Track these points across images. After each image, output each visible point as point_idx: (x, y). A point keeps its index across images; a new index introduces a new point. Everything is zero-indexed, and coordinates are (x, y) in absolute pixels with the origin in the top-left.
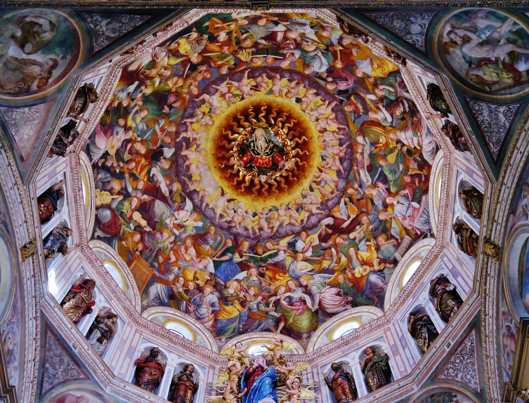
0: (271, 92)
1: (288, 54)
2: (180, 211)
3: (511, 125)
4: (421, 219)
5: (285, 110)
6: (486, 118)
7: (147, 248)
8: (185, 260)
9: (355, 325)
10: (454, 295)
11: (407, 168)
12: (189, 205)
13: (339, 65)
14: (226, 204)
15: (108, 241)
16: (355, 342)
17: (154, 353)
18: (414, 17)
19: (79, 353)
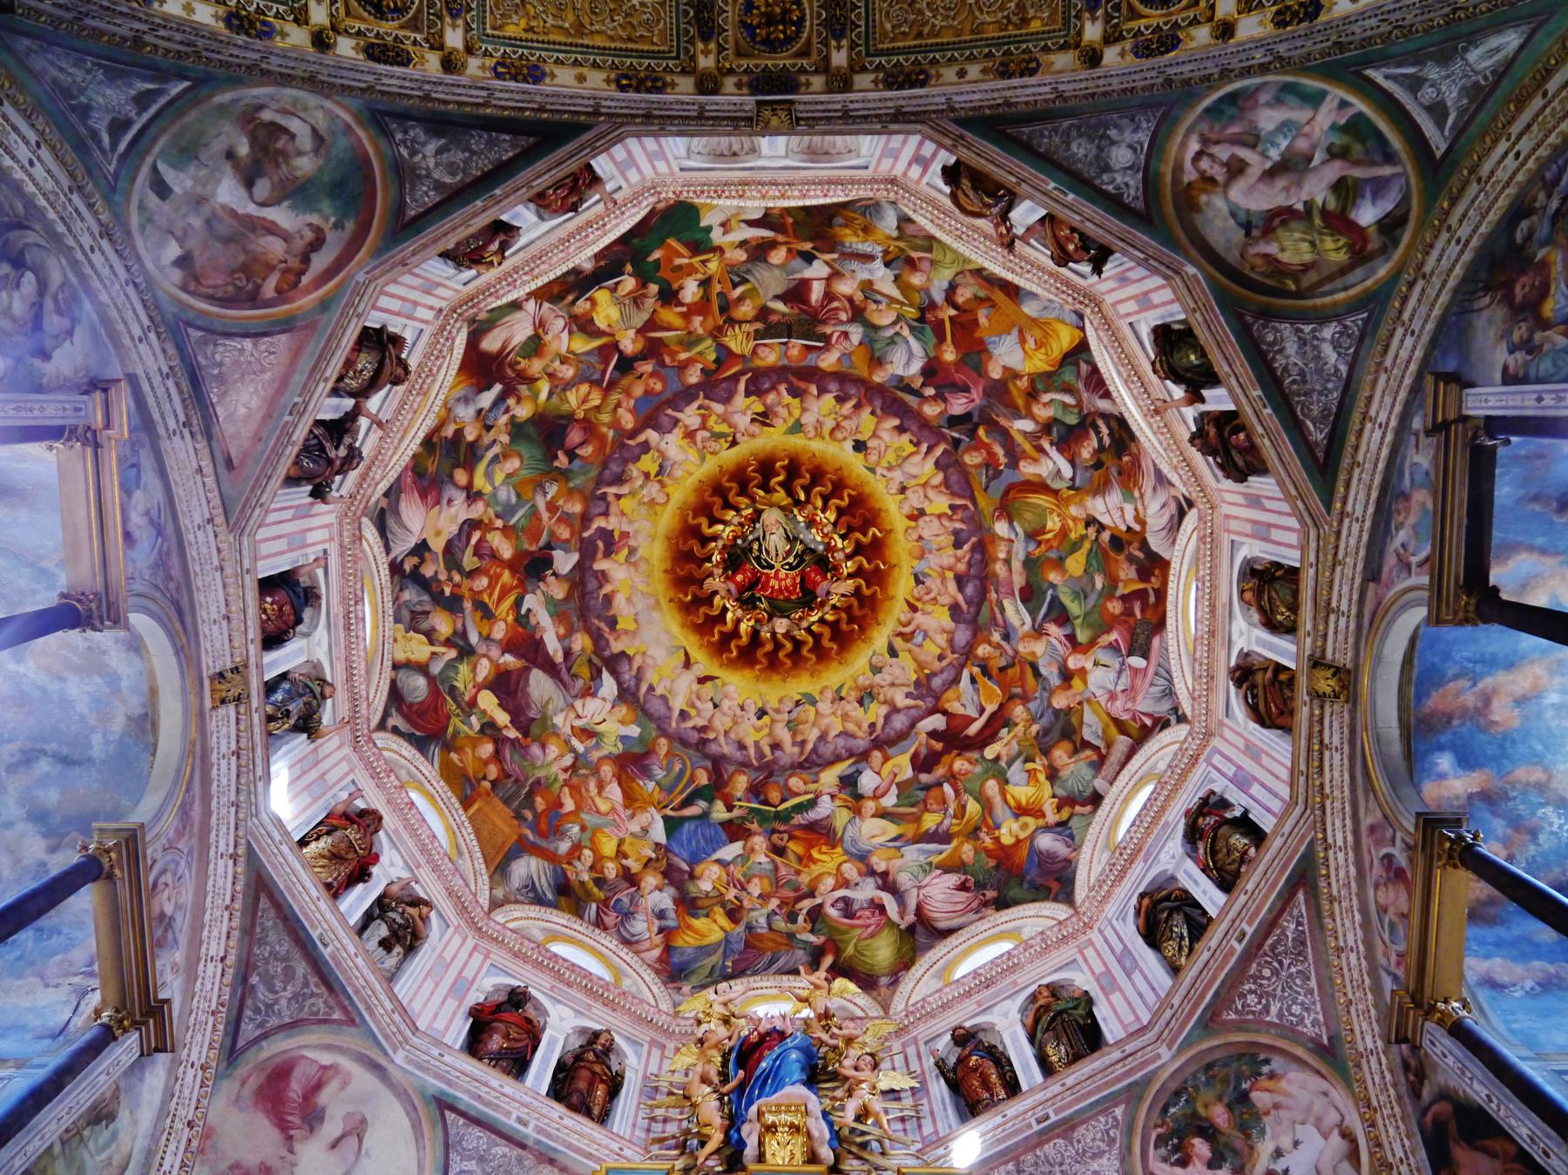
0: (797, 427)
1: (836, 335)
2: (589, 700)
3: (1352, 367)
4: (1154, 690)
5: (829, 469)
6: (1293, 360)
7: (508, 776)
8: (598, 812)
9: (1005, 946)
10: (1245, 824)
11: (1113, 582)
12: (609, 686)
13: (949, 355)
14: (695, 686)
15: (421, 744)
16: (1009, 980)
17: (517, 998)
18: (1116, 127)
19: (334, 957)
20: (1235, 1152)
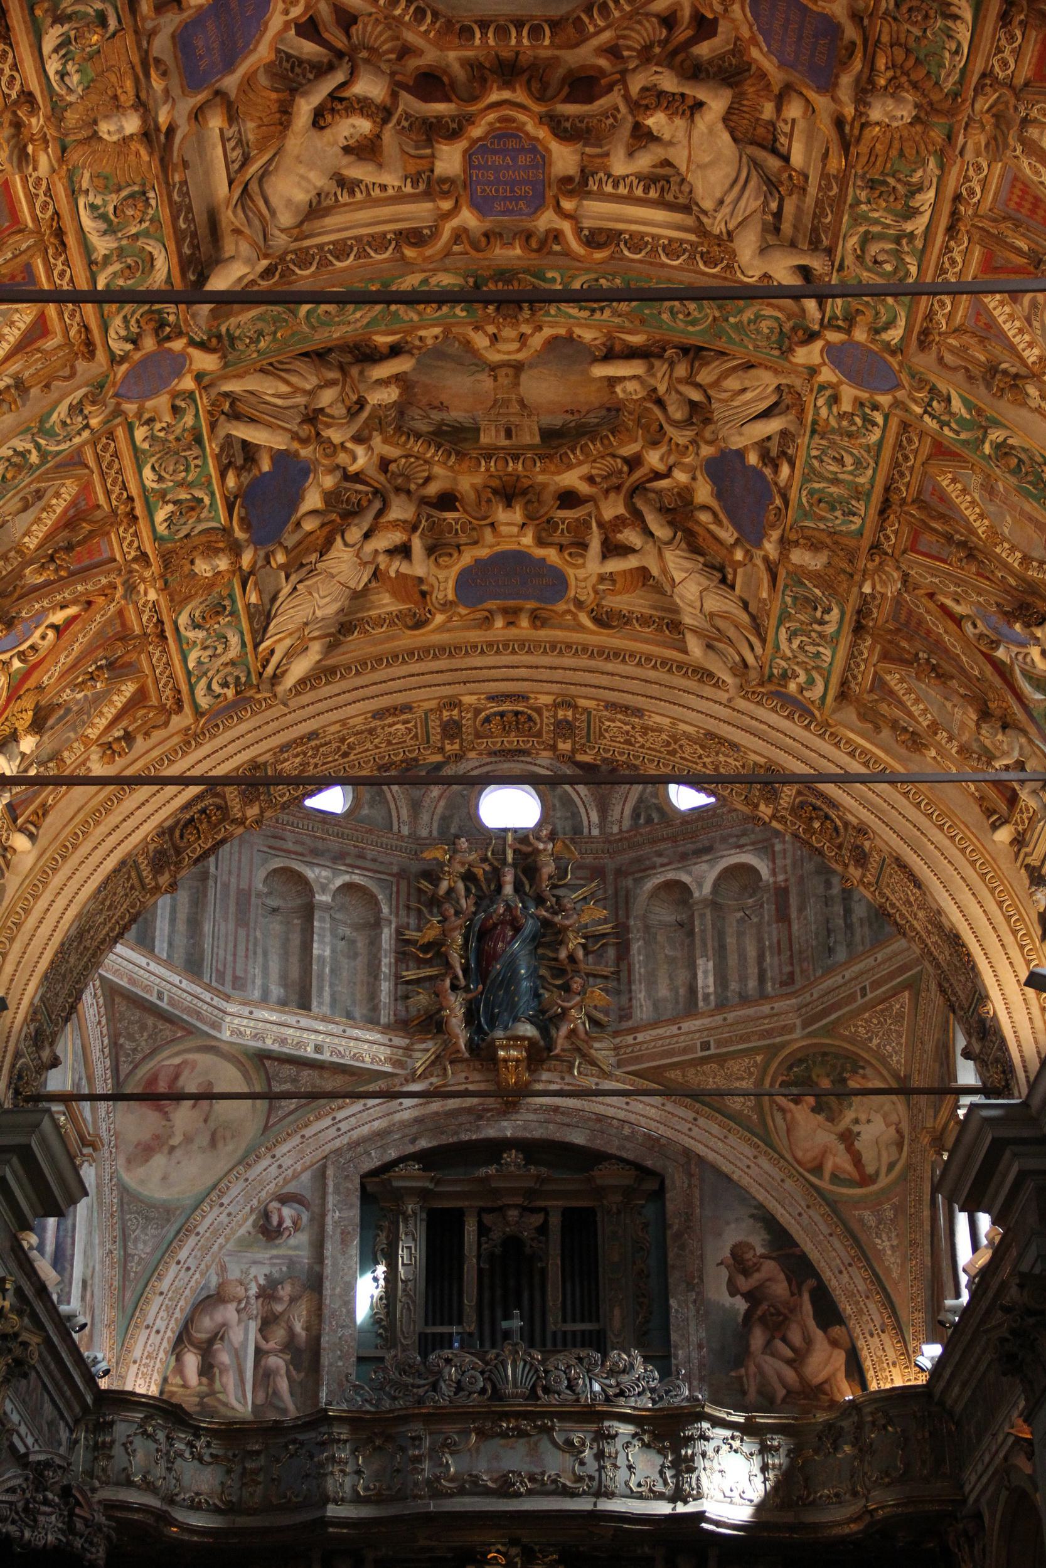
19: (171, 1002)
20: (830, 1109)
